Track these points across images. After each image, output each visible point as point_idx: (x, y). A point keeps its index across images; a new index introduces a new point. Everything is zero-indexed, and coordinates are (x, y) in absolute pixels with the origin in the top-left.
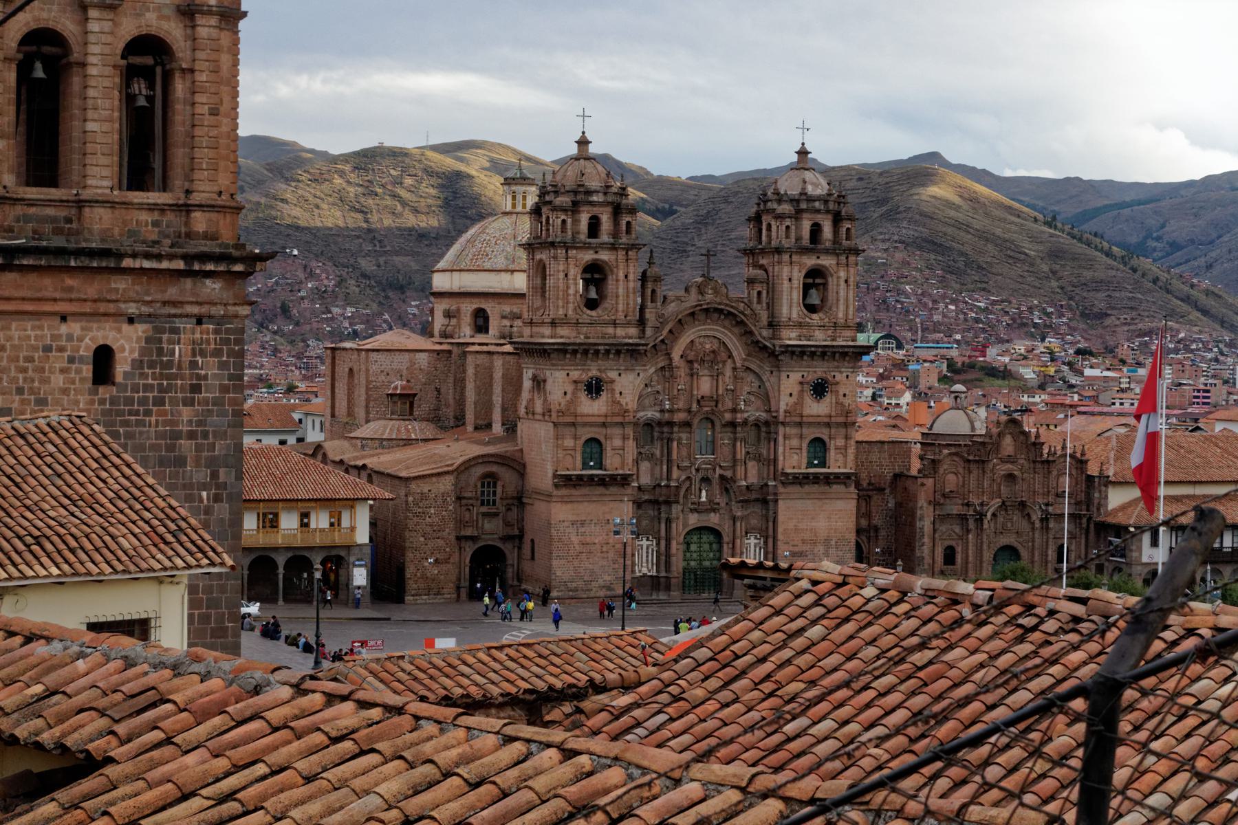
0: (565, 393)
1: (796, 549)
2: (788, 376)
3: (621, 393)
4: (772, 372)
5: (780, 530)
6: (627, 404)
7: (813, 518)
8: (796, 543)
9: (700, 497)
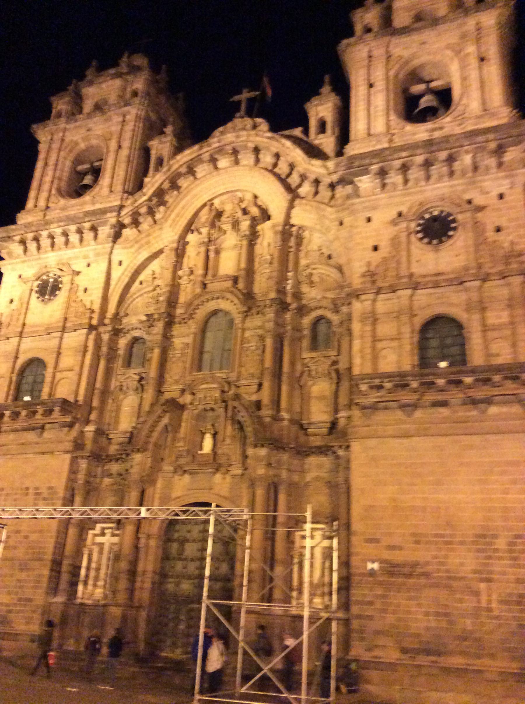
0: (12, 301)
1: (397, 557)
2: (369, 220)
3: (86, 290)
4: (341, 224)
5: (356, 510)
6: (92, 302)
7: (439, 483)
8: (396, 541)
9: (201, 449)
